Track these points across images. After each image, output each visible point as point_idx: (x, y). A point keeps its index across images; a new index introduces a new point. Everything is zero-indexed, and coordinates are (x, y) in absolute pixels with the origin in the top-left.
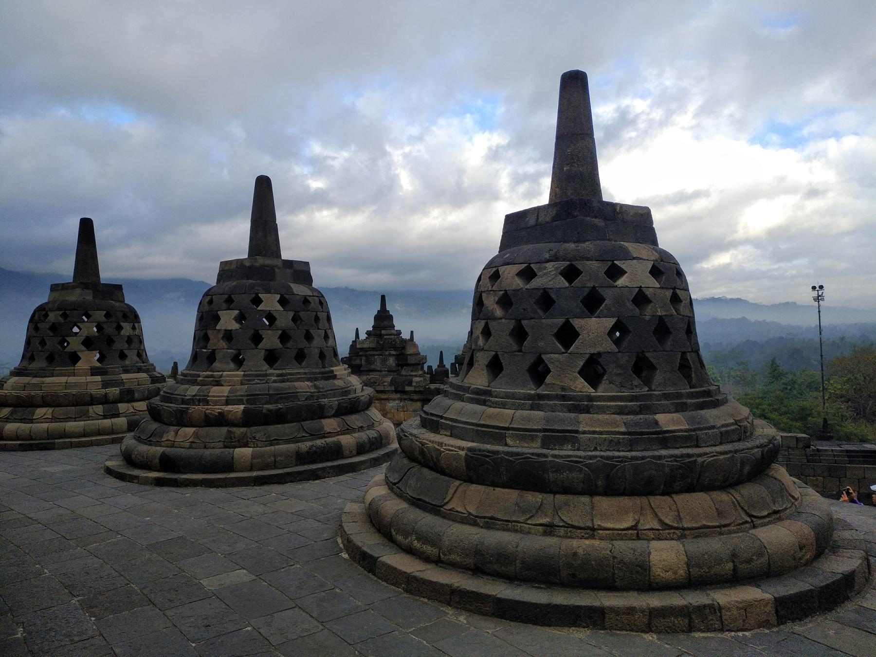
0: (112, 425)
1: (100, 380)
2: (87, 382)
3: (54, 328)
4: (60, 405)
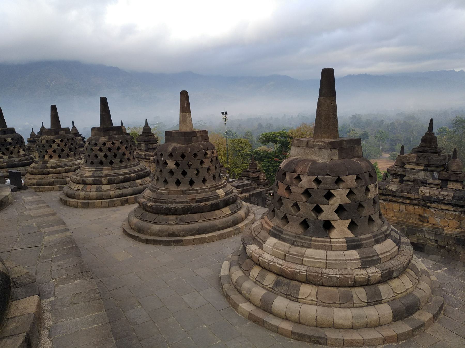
0: (379, 317)
1: (358, 257)
2: (346, 260)
3: (307, 193)
4: (323, 285)
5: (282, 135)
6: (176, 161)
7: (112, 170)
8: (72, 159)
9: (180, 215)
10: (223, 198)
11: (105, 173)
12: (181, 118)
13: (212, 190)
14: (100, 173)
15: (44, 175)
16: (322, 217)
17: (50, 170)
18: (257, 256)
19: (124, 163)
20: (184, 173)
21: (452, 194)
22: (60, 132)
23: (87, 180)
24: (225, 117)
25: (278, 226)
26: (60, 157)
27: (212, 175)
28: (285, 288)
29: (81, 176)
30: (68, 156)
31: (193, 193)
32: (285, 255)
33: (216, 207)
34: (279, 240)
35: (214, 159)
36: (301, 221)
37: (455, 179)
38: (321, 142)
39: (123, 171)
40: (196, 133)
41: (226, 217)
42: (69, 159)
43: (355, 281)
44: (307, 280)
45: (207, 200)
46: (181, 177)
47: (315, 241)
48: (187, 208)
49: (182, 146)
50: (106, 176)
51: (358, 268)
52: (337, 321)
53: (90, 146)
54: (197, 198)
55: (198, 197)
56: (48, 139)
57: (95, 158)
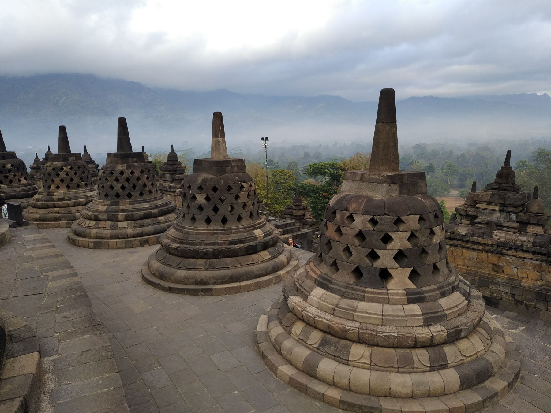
0: (444, 385)
1: (420, 313)
2: (406, 316)
3: (361, 235)
5: (332, 166)
6: (206, 195)
7: (130, 204)
8: (82, 190)
9: (209, 258)
10: (262, 240)
11: (122, 207)
12: (214, 144)
13: (249, 230)
14: (115, 208)
15: (49, 210)
16: (379, 264)
17: (56, 203)
18: (300, 309)
19: (144, 196)
20: (216, 210)
21: (531, 239)
22: (69, 158)
23: (100, 215)
24: (266, 143)
25: (326, 275)
26: (68, 187)
27: (249, 213)
28: (333, 348)
29: (93, 211)
30: (78, 186)
31: (226, 233)
32: (334, 309)
33: (252, 250)
34: (327, 290)
35: (252, 193)
36: (353, 269)
37: (535, 222)
38: (379, 175)
39: (142, 206)
40: (231, 162)
41: (265, 262)
42: (80, 190)
43: (416, 341)
44: (359, 338)
45: (242, 241)
46: (211, 214)
47: (369, 292)
48: (219, 251)
49: (215, 177)
50: (123, 211)
51: (420, 326)
52: (395, 388)
53: (105, 175)
54: (230, 239)
55: (232, 237)
56: (55, 166)
57: (110, 190)
